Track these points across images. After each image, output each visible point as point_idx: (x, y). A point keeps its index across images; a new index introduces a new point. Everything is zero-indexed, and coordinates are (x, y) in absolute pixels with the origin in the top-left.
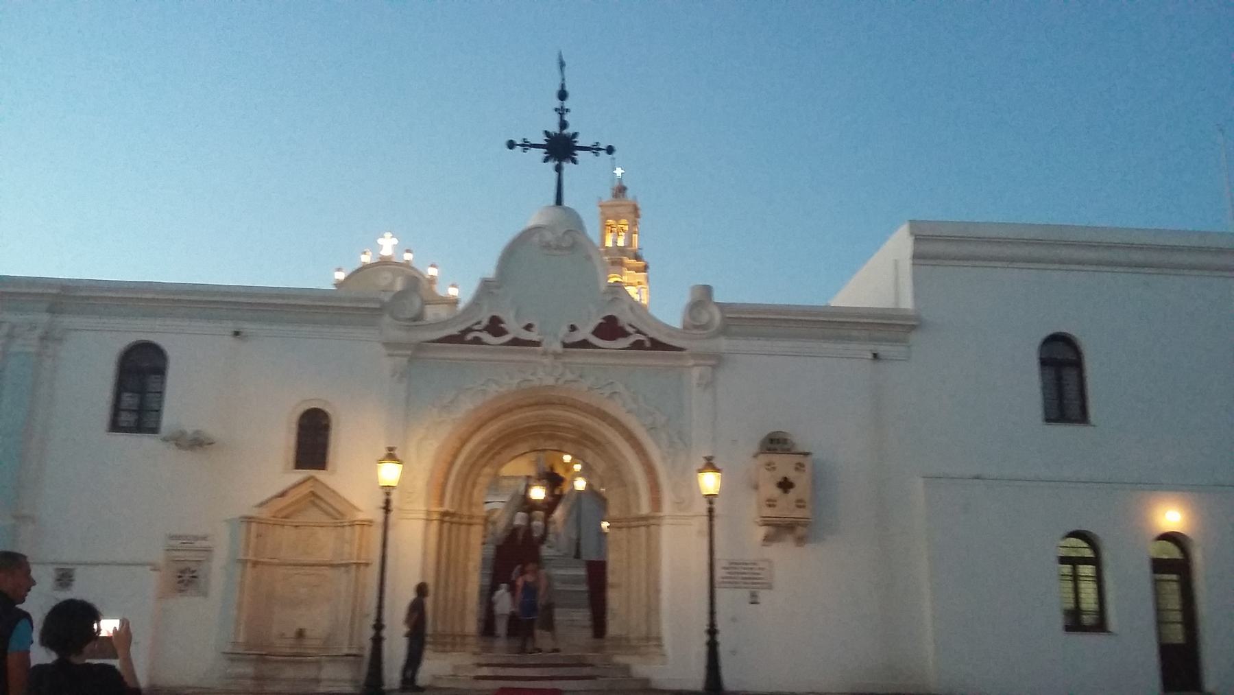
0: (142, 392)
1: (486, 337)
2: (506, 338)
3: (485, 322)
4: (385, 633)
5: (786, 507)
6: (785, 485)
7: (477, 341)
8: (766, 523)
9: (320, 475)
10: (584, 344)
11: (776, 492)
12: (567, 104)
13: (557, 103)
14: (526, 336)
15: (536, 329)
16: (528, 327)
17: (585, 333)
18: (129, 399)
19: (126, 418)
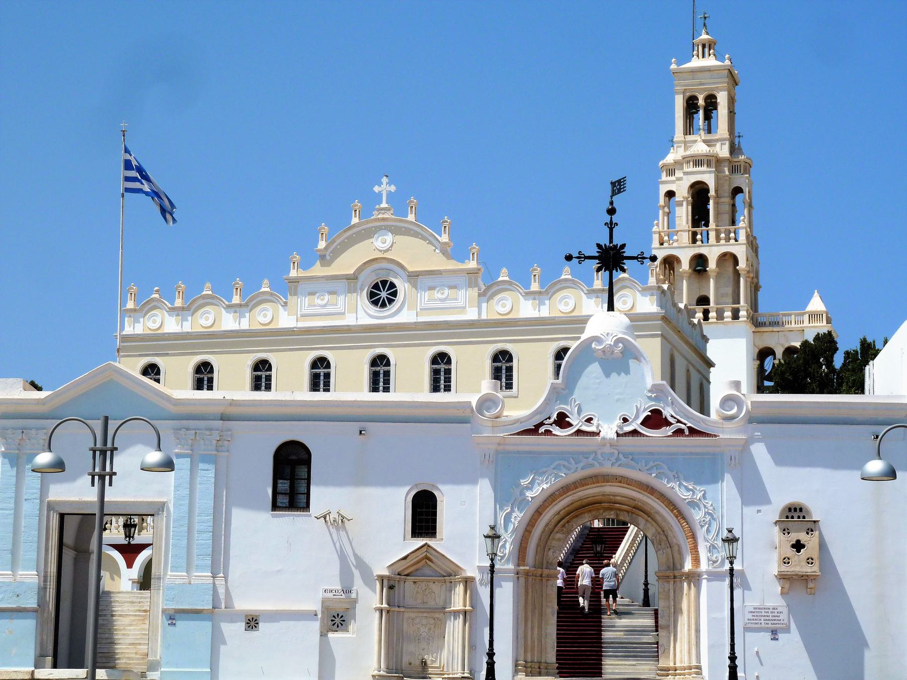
0: (293, 480)
1: (556, 430)
2: (572, 430)
3: (554, 417)
4: (495, 658)
5: (799, 565)
6: (798, 546)
7: (548, 432)
8: (782, 577)
9: (431, 542)
10: (635, 433)
11: (791, 552)
12: (615, 218)
13: (607, 218)
14: (585, 428)
15: (595, 422)
16: (589, 420)
17: (635, 425)
18: (284, 485)
19: (283, 500)
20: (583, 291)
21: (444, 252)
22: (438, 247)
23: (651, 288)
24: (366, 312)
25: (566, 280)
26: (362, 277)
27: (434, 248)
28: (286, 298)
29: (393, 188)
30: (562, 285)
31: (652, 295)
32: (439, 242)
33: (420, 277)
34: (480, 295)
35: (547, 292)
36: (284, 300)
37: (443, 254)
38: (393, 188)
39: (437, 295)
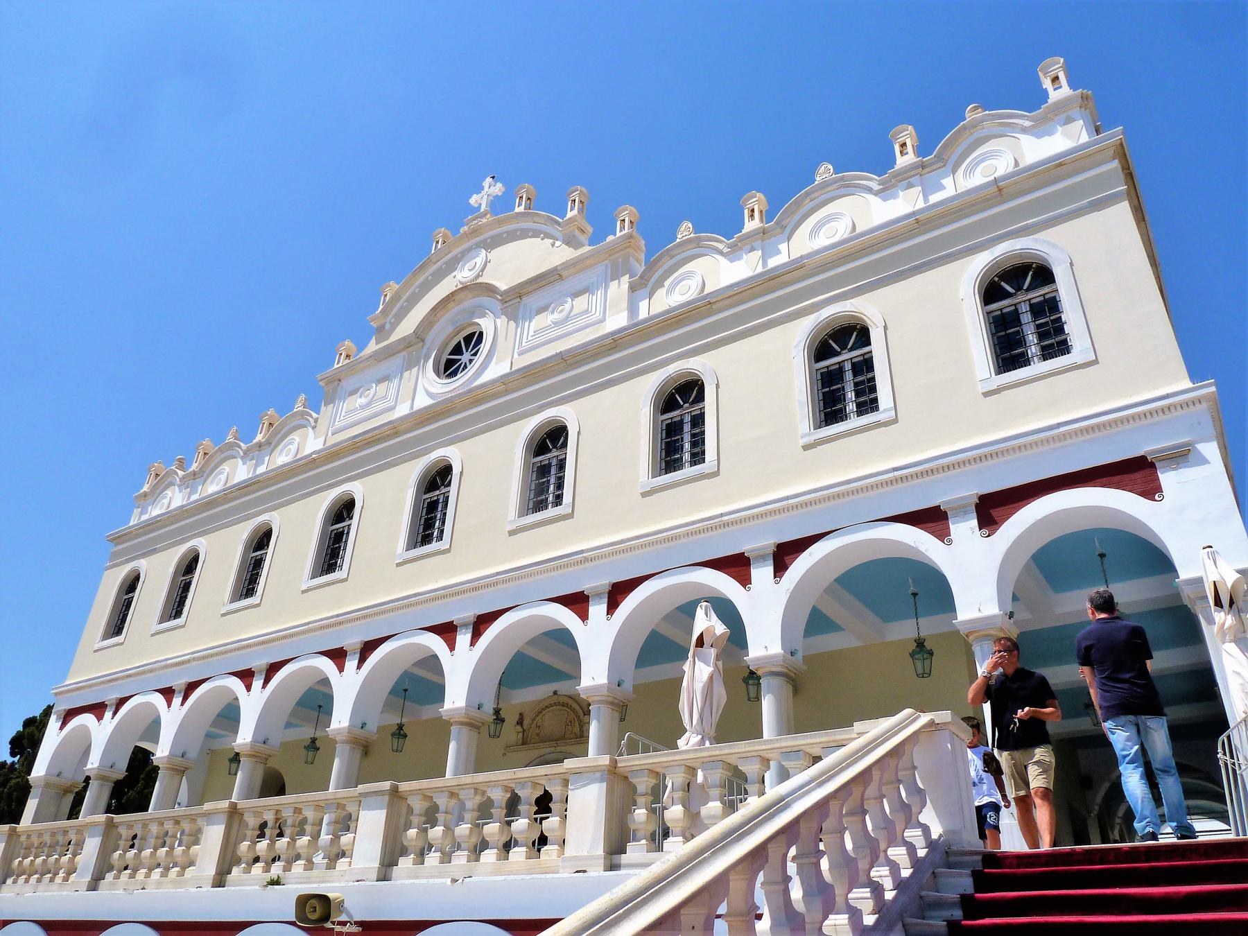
20: (869, 190)
21: (570, 242)
22: (559, 235)
23: (1062, 105)
24: (427, 391)
25: (824, 185)
26: (429, 338)
27: (551, 241)
28: (318, 413)
29: (498, 189)
30: (812, 204)
31: (1069, 121)
32: (558, 223)
33: (524, 299)
34: (633, 288)
35: (781, 226)
36: (315, 415)
37: (566, 244)
38: (498, 189)
39: (548, 318)
